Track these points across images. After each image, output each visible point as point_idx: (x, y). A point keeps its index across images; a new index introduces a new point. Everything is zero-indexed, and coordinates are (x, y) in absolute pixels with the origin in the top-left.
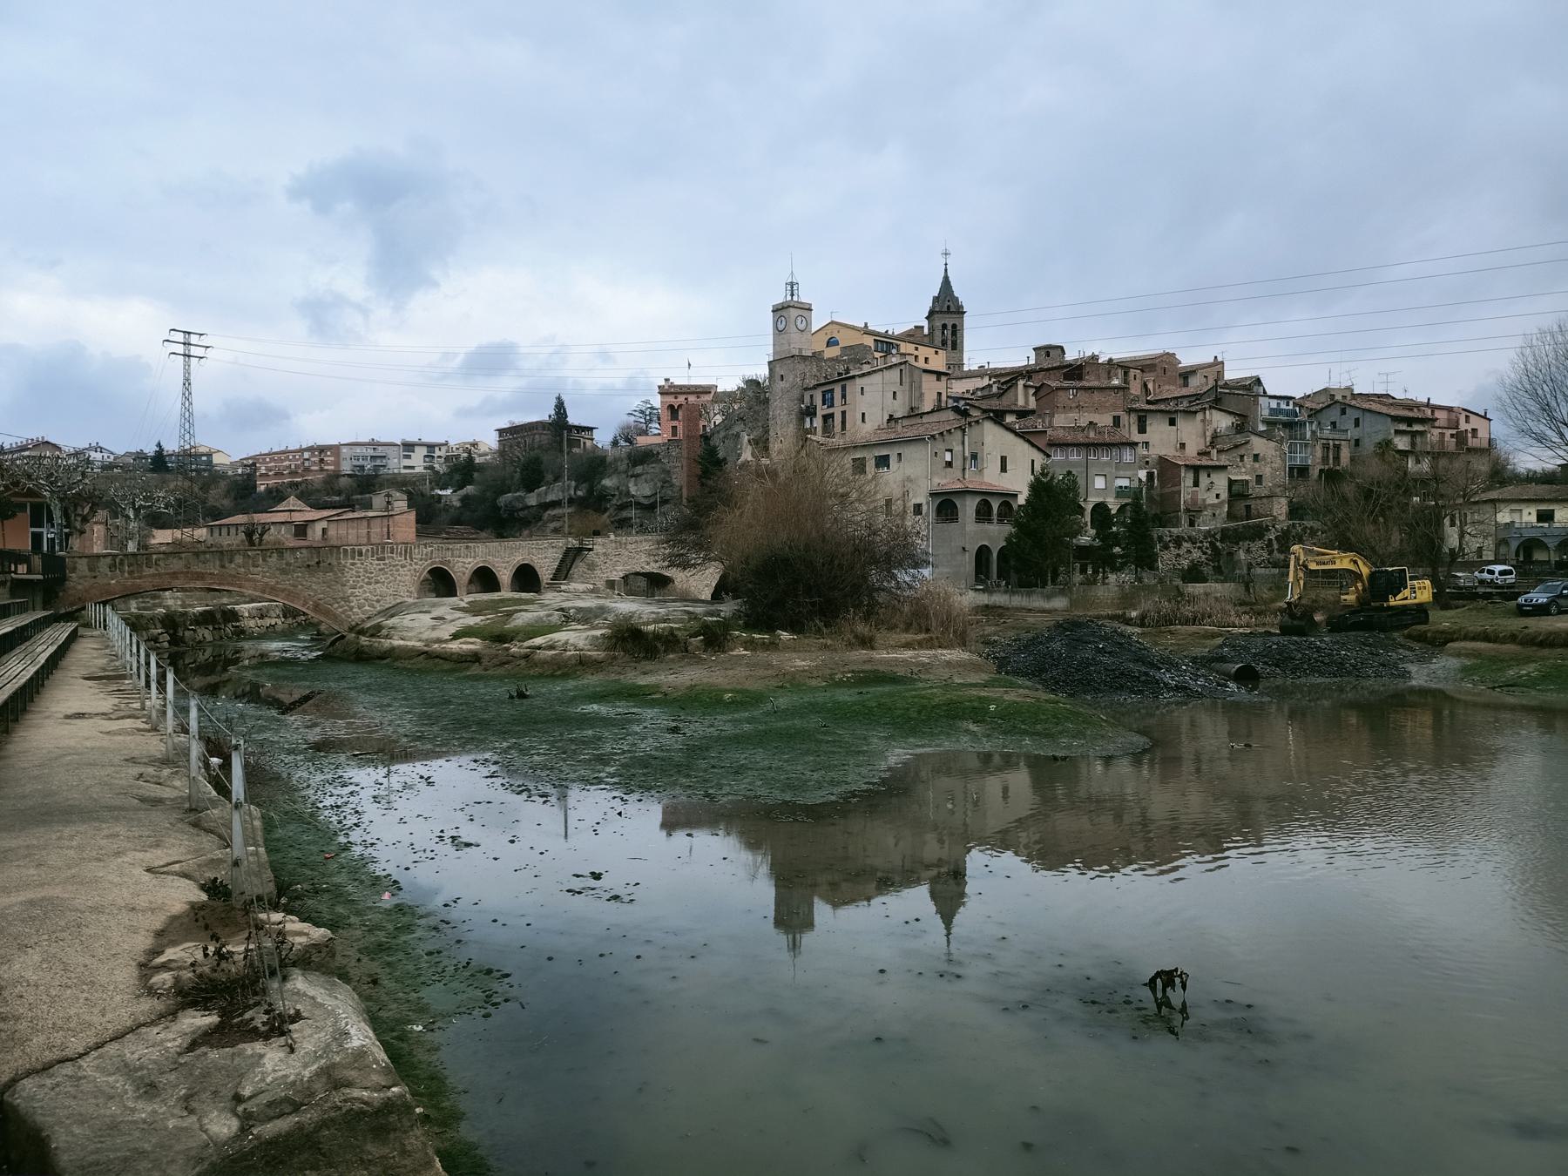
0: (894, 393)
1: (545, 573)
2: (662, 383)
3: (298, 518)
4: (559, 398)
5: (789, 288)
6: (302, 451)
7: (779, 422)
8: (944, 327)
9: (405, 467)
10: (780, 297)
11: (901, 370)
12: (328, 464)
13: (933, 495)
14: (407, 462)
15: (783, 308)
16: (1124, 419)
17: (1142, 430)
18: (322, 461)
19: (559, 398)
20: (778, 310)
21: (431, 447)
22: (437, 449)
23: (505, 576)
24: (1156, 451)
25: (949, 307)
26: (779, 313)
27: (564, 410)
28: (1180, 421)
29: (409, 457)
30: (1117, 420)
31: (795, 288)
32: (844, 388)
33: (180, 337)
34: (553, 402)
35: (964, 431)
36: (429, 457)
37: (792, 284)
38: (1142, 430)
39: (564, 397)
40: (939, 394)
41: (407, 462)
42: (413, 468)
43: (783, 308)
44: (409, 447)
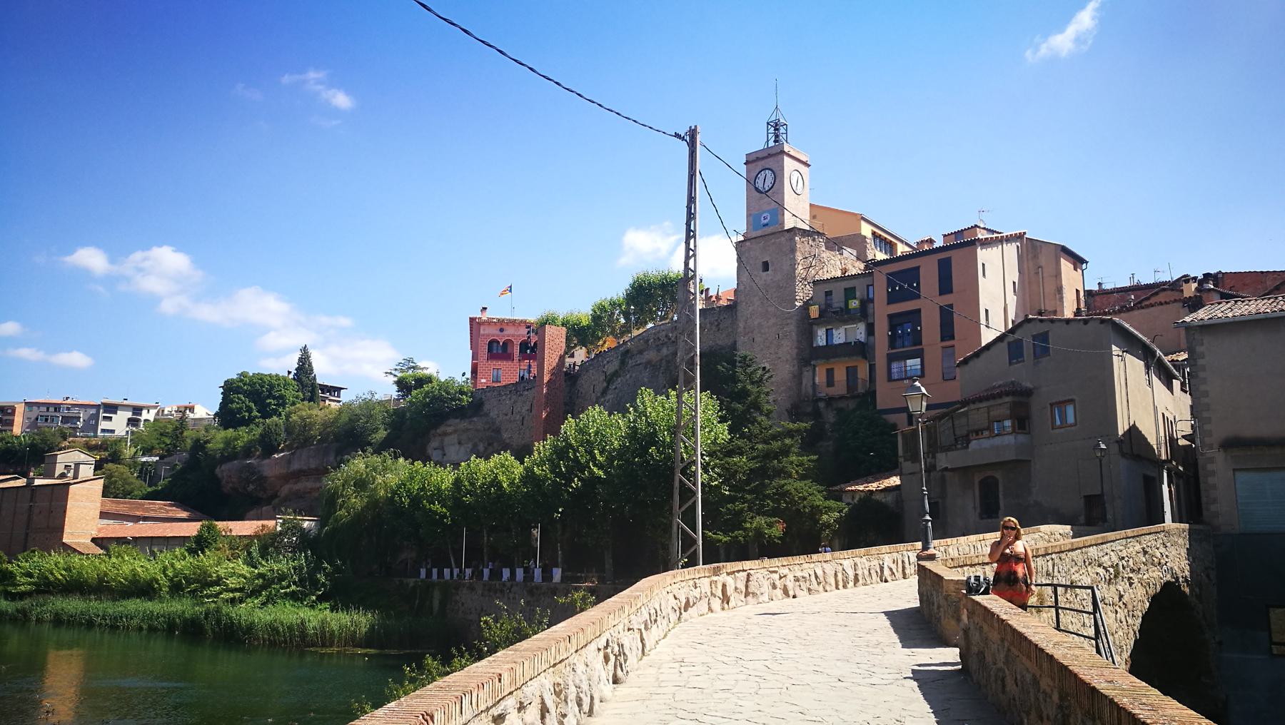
2: (478, 315)
4: (305, 350)
5: (772, 130)
7: (758, 339)
9: (103, 431)
10: (758, 141)
15: (770, 156)
19: (305, 350)
20: (751, 160)
21: (137, 410)
22: (144, 412)
26: (761, 164)
29: (110, 419)
31: (782, 130)
34: (298, 355)
36: (132, 422)
37: (777, 126)
42: (113, 431)
43: (770, 156)
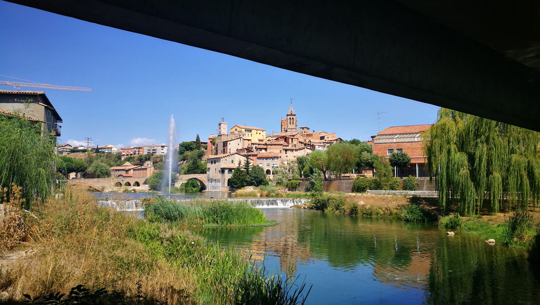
0: (239, 144)
1: (141, 183)
3: (127, 168)
6: (134, 148)
8: (290, 118)
9: (162, 152)
11: (240, 139)
12: (141, 152)
13: (221, 168)
14: (162, 151)
16: (282, 151)
17: (286, 153)
18: (139, 151)
23: (132, 184)
24: (288, 158)
25: (291, 113)
27: (199, 138)
28: (294, 151)
30: (281, 151)
32: (226, 143)
33: (87, 139)
34: (196, 136)
35: (229, 156)
38: (286, 153)
39: (199, 135)
40: (249, 144)
41: (162, 151)
44: (163, 147)
